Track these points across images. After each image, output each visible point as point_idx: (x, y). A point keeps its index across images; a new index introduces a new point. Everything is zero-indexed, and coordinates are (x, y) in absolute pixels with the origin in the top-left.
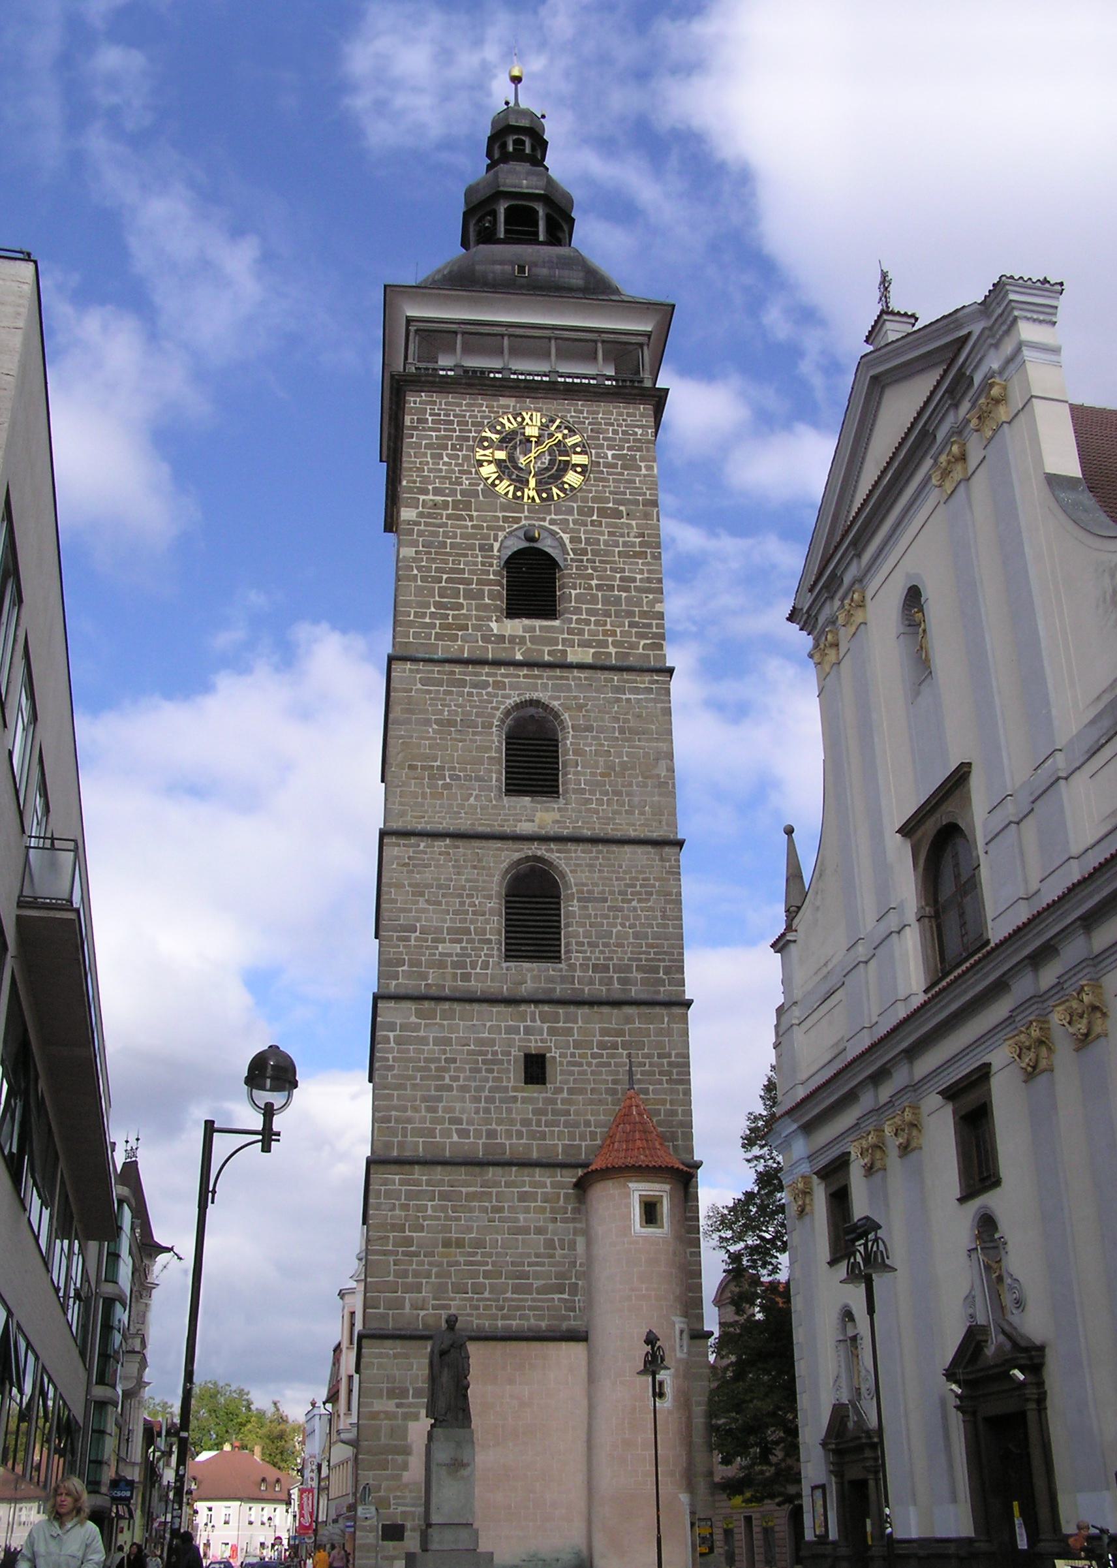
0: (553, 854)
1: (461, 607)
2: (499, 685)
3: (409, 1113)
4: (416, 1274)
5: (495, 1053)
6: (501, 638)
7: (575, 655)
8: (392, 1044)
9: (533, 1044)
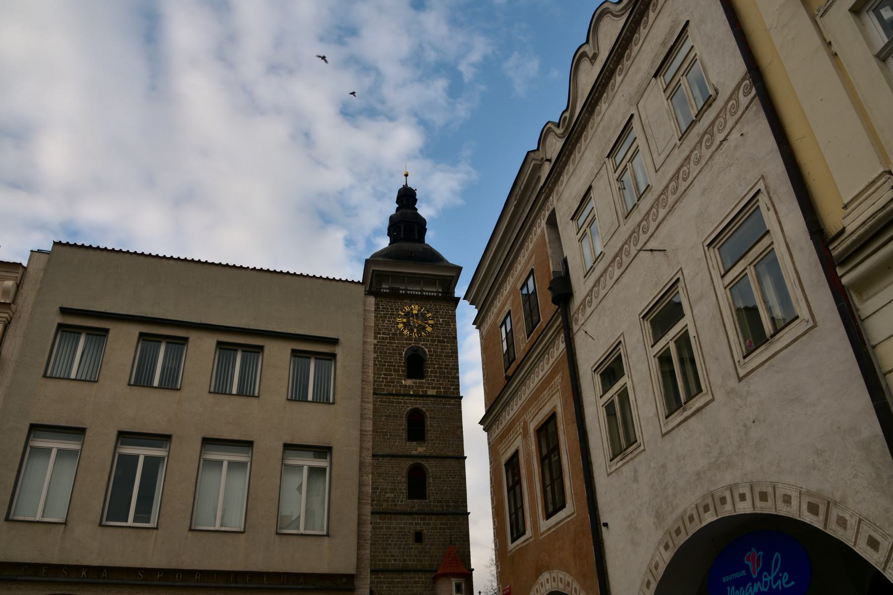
0: (424, 462)
2: (405, 403)
6: (405, 386)
7: (431, 392)
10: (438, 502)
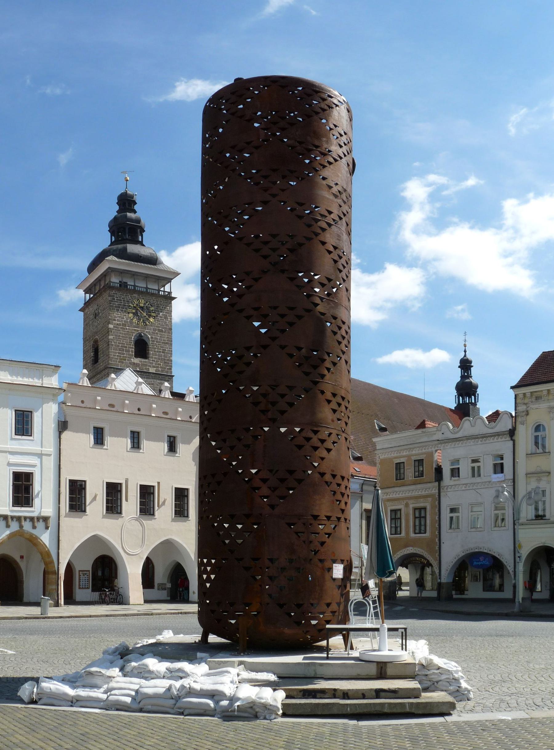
1: (124, 354)
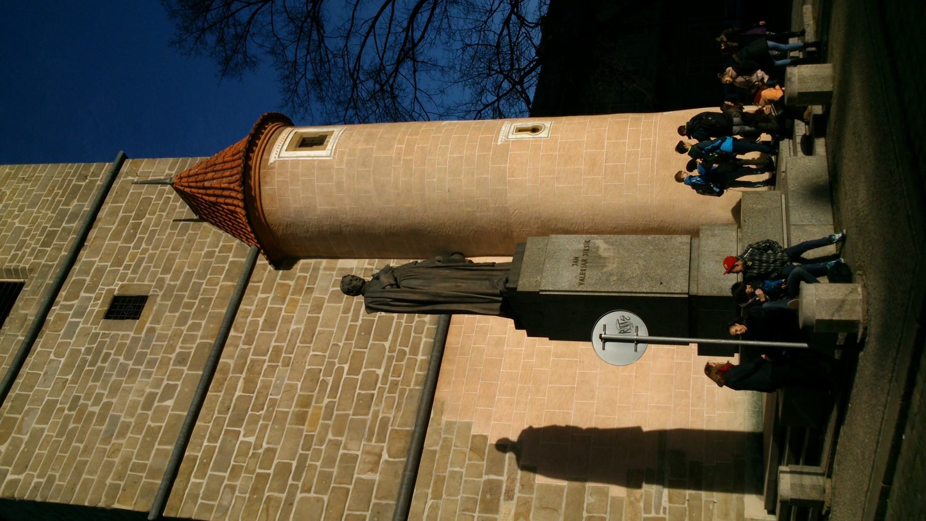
3: (117, 460)
4: (330, 461)
5: (88, 351)
8: (22, 477)
9: (97, 309)
10: (46, 244)
